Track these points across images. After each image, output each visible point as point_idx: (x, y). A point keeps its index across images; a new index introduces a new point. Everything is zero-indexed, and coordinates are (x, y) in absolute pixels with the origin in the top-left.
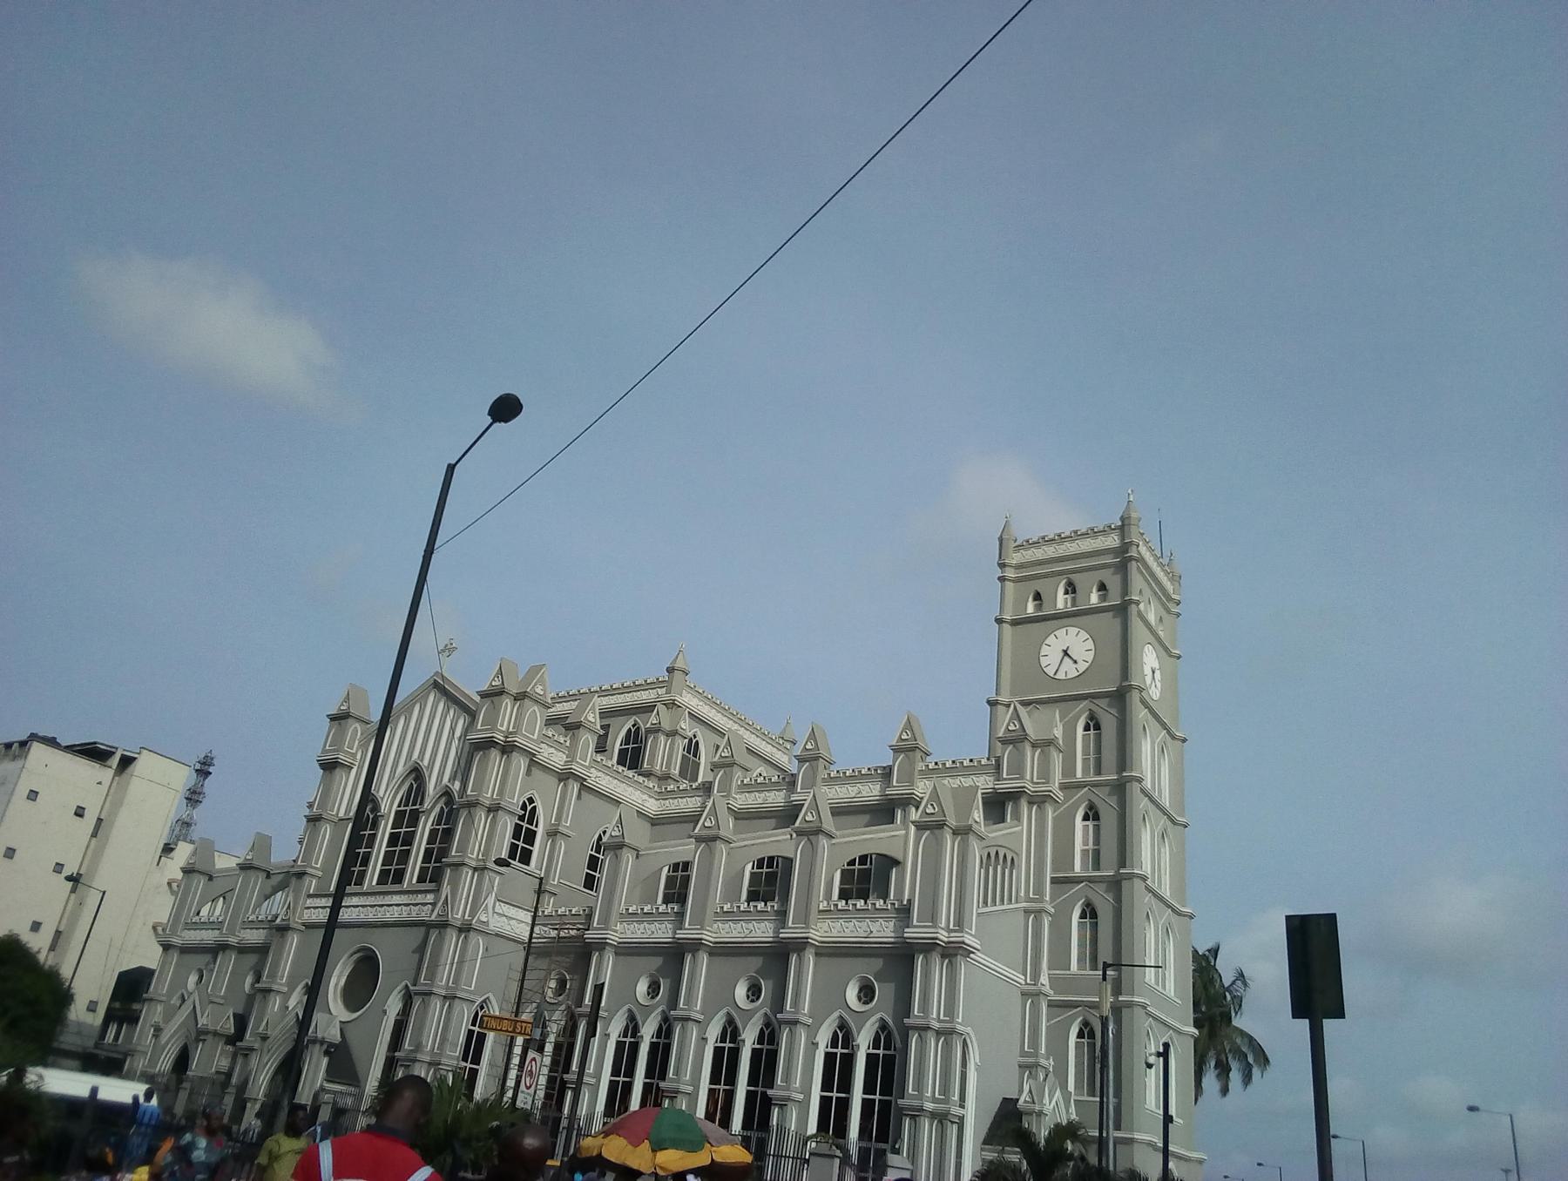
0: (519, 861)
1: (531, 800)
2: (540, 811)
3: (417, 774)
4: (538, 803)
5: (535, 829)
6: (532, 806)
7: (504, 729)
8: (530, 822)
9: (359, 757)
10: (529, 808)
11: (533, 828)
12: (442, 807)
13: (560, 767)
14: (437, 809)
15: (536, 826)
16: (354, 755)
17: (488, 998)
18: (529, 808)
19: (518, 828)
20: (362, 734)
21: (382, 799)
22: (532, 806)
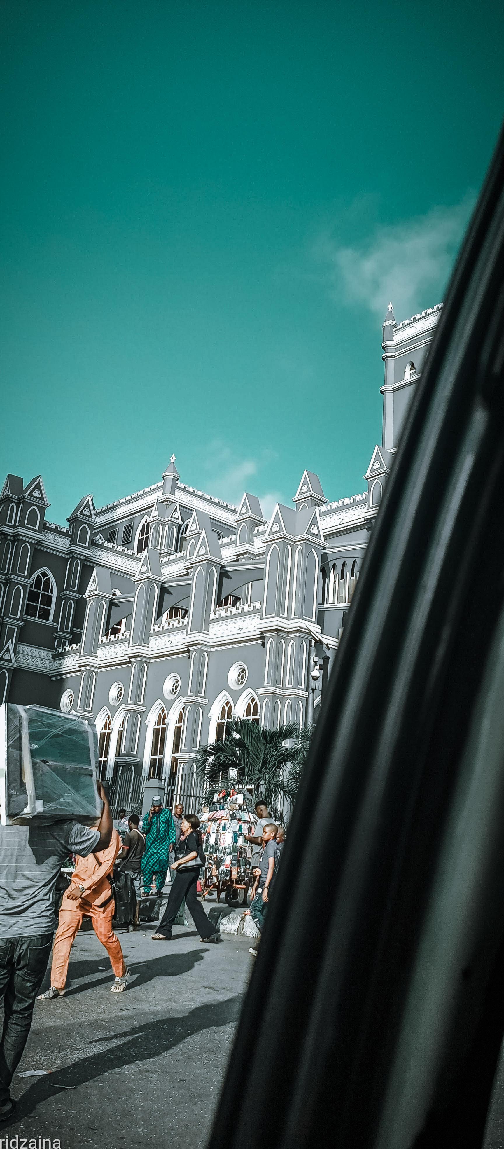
1: (44, 575)
2: (53, 581)
4: (51, 575)
5: (51, 595)
7: (13, 524)
8: (46, 589)
11: (49, 594)
13: (66, 550)
15: (52, 592)
19: (33, 596)
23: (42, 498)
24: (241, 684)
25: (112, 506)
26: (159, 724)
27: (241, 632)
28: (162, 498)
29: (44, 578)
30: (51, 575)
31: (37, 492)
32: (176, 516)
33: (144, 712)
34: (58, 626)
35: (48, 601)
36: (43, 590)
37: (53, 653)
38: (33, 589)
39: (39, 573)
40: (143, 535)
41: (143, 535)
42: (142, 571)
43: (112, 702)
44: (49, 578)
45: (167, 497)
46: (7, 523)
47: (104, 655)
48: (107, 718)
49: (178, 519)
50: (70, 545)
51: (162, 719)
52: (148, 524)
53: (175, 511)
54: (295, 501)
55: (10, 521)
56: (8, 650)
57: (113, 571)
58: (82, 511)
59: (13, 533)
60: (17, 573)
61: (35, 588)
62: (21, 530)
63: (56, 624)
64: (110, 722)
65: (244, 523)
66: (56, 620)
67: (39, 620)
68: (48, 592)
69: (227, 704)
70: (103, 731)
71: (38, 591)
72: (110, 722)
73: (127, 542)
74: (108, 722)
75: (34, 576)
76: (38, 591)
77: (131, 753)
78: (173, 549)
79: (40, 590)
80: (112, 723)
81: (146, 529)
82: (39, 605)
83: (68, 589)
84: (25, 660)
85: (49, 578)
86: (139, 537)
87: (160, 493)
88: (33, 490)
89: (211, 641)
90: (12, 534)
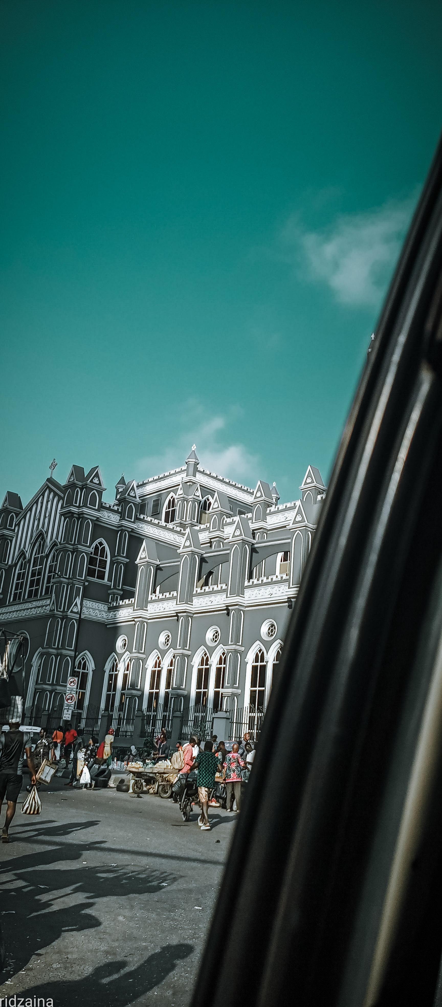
0: (97, 578)
1: (101, 544)
2: (107, 549)
3: (41, 536)
5: (106, 559)
6: (102, 547)
7: (78, 505)
9: (16, 531)
10: (100, 548)
11: (104, 559)
12: (54, 553)
14: (52, 554)
15: (106, 558)
16: (14, 530)
17: (85, 653)
18: (100, 548)
19: (92, 561)
20: (16, 518)
21: (27, 552)
22: (102, 547)
23: (100, 484)
24: (271, 636)
25: (142, 483)
26: (202, 665)
27: (272, 596)
28: (186, 479)
29: (100, 547)
30: (105, 545)
31: (96, 479)
32: (197, 494)
33: (190, 655)
34: (111, 584)
35: (103, 564)
36: (100, 556)
37: (109, 606)
38: (92, 556)
39: (97, 543)
40: (169, 508)
41: (169, 508)
42: (186, 545)
43: (161, 646)
44: (104, 547)
45: (190, 479)
46: (74, 504)
47: (154, 610)
48: (156, 658)
49: (199, 496)
50: (120, 520)
51: (205, 661)
52: (174, 500)
53: (196, 490)
54: (302, 490)
55: (76, 503)
56: (76, 605)
57: (157, 541)
58: (129, 493)
59: (78, 512)
60: (82, 543)
61: (94, 555)
62: (85, 510)
63: (110, 583)
64: (160, 662)
65: (258, 505)
66: (110, 580)
67: (98, 580)
68: (104, 558)
69: (260, 651)
70: (154, 669)
71: (97, 557)
72: (160, 662)
73: (156, 513)
74: (158, 661)
75: (94, 545)
76: (97, 557)
77: (181, 687)
78: (196, 521)
79: (98, 556)
80: (162, 663)
81: (172, 503)
82: (97, 568)
83: (119, 555)
84: (87, 612)
85: (104, 547)
86: (166, 509)
87: (184, 475)
88: (93, 478)
89: (246, 602)
90: (77, 513)
